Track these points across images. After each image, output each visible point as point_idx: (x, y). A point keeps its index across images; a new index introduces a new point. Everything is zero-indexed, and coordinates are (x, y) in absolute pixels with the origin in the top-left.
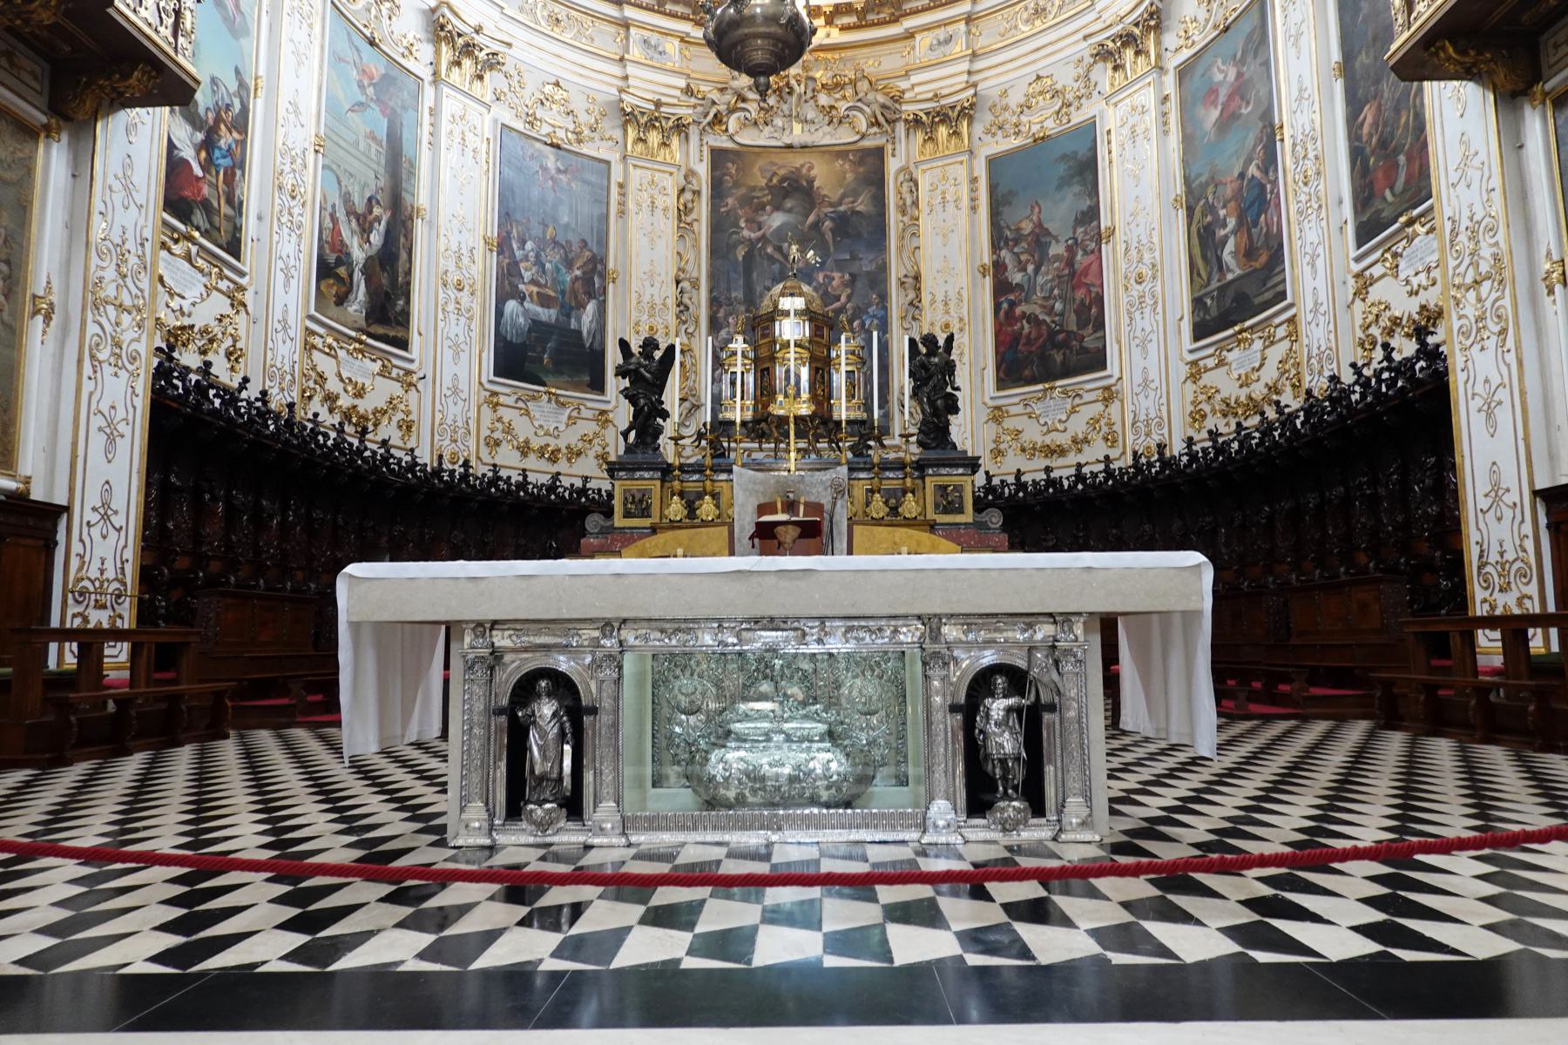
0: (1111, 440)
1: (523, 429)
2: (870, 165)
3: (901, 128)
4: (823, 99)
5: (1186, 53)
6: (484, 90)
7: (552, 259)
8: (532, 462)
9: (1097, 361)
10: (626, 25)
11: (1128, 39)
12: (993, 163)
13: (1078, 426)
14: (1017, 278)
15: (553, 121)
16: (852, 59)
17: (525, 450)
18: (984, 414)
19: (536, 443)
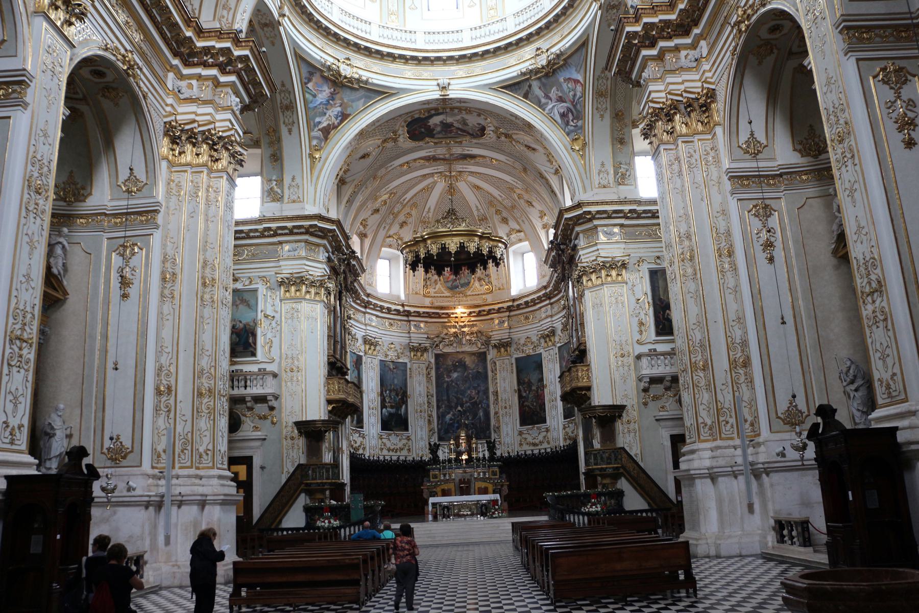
0: (548, 443)
1: (388, 444)
2: (482, 356)
3: (491, 348)
4: (468, 337)
5: (559, 345)
6: (375, 353)
7: (393, 394)
8: (391, 453)
9: (545, 421)
10: (409, 321)
11: (548, 336)
12: (517, 359)
13: (541, 438)
14: (524, 394)
15: (392, 355)
16: (475, 325)
17: (389, 450)
18: (516, 433)
19: (392, 448)
